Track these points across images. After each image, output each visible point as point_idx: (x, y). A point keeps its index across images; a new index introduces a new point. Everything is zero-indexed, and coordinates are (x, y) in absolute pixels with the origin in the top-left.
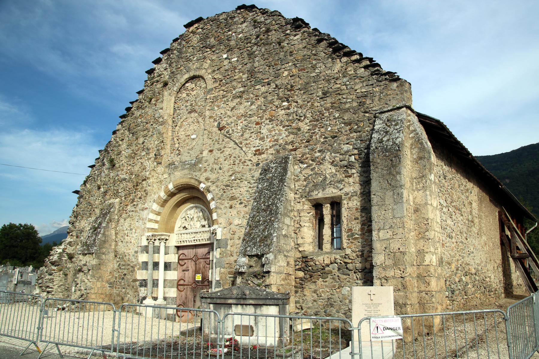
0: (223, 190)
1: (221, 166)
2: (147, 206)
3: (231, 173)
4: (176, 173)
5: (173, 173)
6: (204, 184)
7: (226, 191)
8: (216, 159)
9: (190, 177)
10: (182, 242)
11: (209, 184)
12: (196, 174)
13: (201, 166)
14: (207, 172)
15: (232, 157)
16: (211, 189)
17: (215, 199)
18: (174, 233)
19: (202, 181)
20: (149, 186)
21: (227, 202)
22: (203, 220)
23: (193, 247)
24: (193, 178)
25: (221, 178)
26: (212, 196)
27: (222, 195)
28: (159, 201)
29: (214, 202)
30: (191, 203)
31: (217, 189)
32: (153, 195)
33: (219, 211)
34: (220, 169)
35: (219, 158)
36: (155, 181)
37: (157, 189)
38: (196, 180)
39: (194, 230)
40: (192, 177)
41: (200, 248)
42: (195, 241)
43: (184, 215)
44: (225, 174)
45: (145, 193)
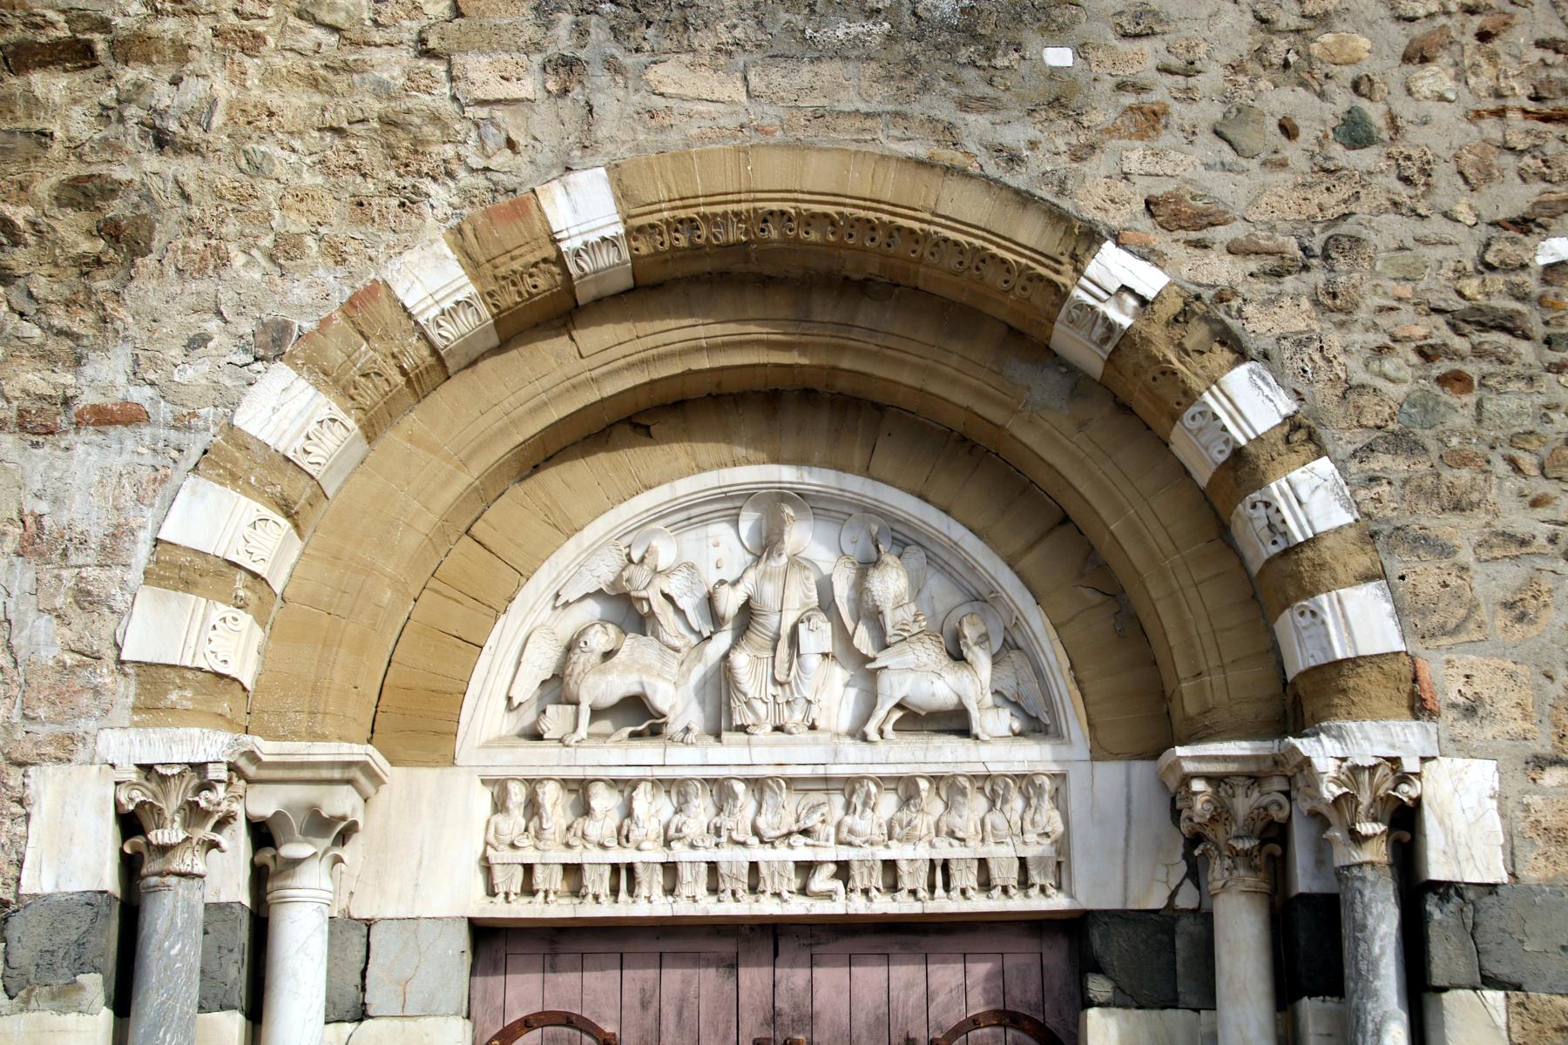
0: (1427, 354)
1: (1375, 113)
2: (141, 395)
3: (1517, 197)
4: (670, 75)
5: (613, 67)
6: (1149, 255)
7: (1472, 369)
8: (1288, 17)
9: (919, 150)
10: (651, 883)
11: (1220, 269)
12: (1015, 135)
13: (1059, 57)
14: (1166, 139)
15: (1521, 36)
16: (1258, 326)
17: (1344, 439)
18: (452, 762)
19: (1116, 219)
20: (161, 141)
21: (1514, 483)
22: (929, 654)
23: (726, 947)
24: (965, 174)
25: (1388, 230)
26: (1287, 405)
27: (1426, 407)
28: (366, 353)
29: (1324, 465)
30: (754, 443)
31: (1335, 340)
32: (248, 271)
33: (1426, 575)
34: (1355, 133)
35: (1323, 20)
36: (296, 102)
37: (334, 210)
38: (1025, 199)
39: (802, 755)
40: (947, 155)
41: (887, 959)
42: (821, 881)
43: (603, 571)
44: (1444, 201)
45: (84, 219)
